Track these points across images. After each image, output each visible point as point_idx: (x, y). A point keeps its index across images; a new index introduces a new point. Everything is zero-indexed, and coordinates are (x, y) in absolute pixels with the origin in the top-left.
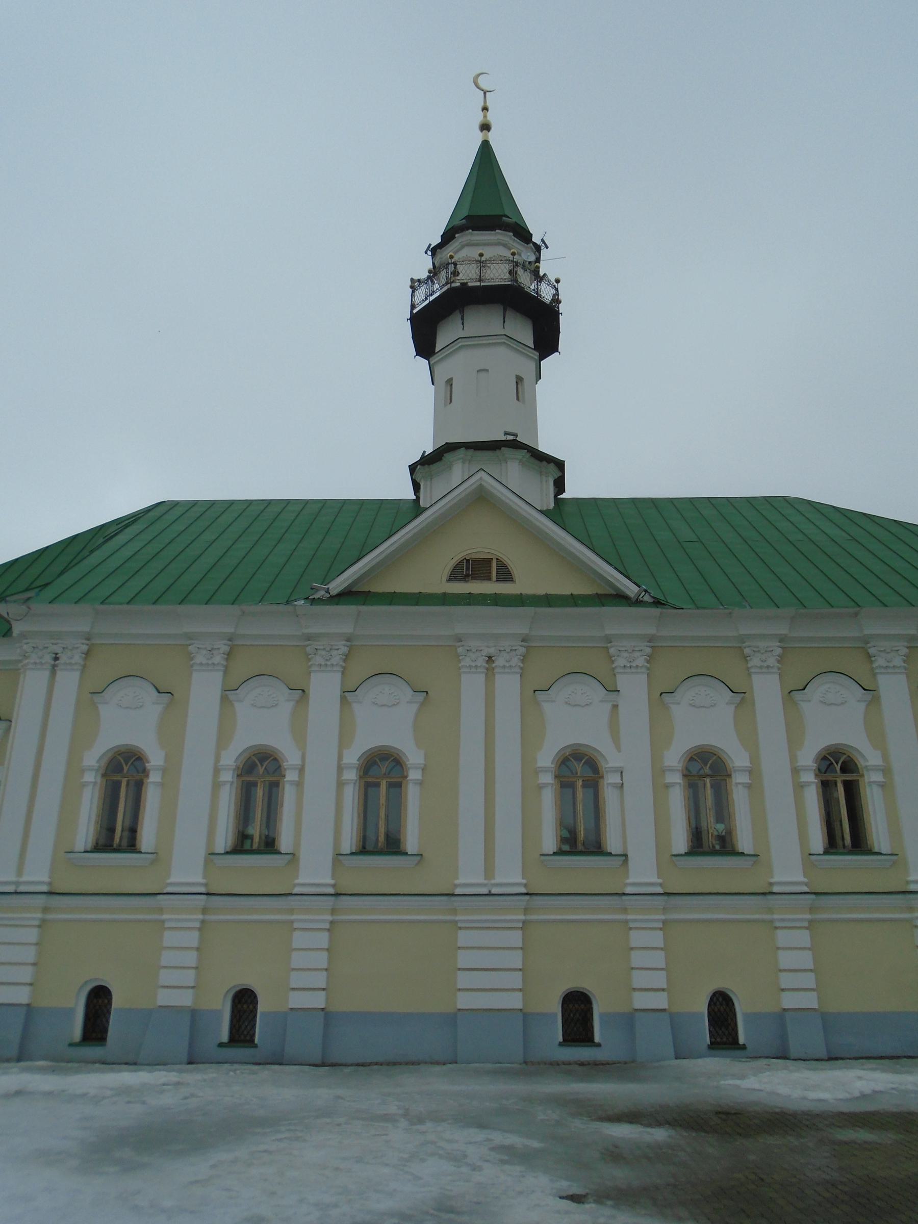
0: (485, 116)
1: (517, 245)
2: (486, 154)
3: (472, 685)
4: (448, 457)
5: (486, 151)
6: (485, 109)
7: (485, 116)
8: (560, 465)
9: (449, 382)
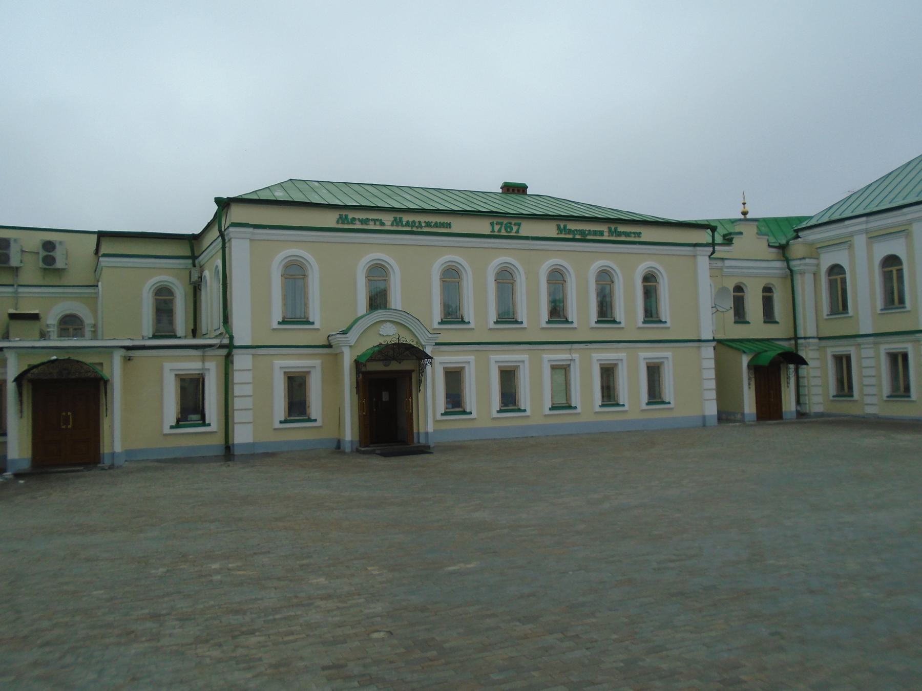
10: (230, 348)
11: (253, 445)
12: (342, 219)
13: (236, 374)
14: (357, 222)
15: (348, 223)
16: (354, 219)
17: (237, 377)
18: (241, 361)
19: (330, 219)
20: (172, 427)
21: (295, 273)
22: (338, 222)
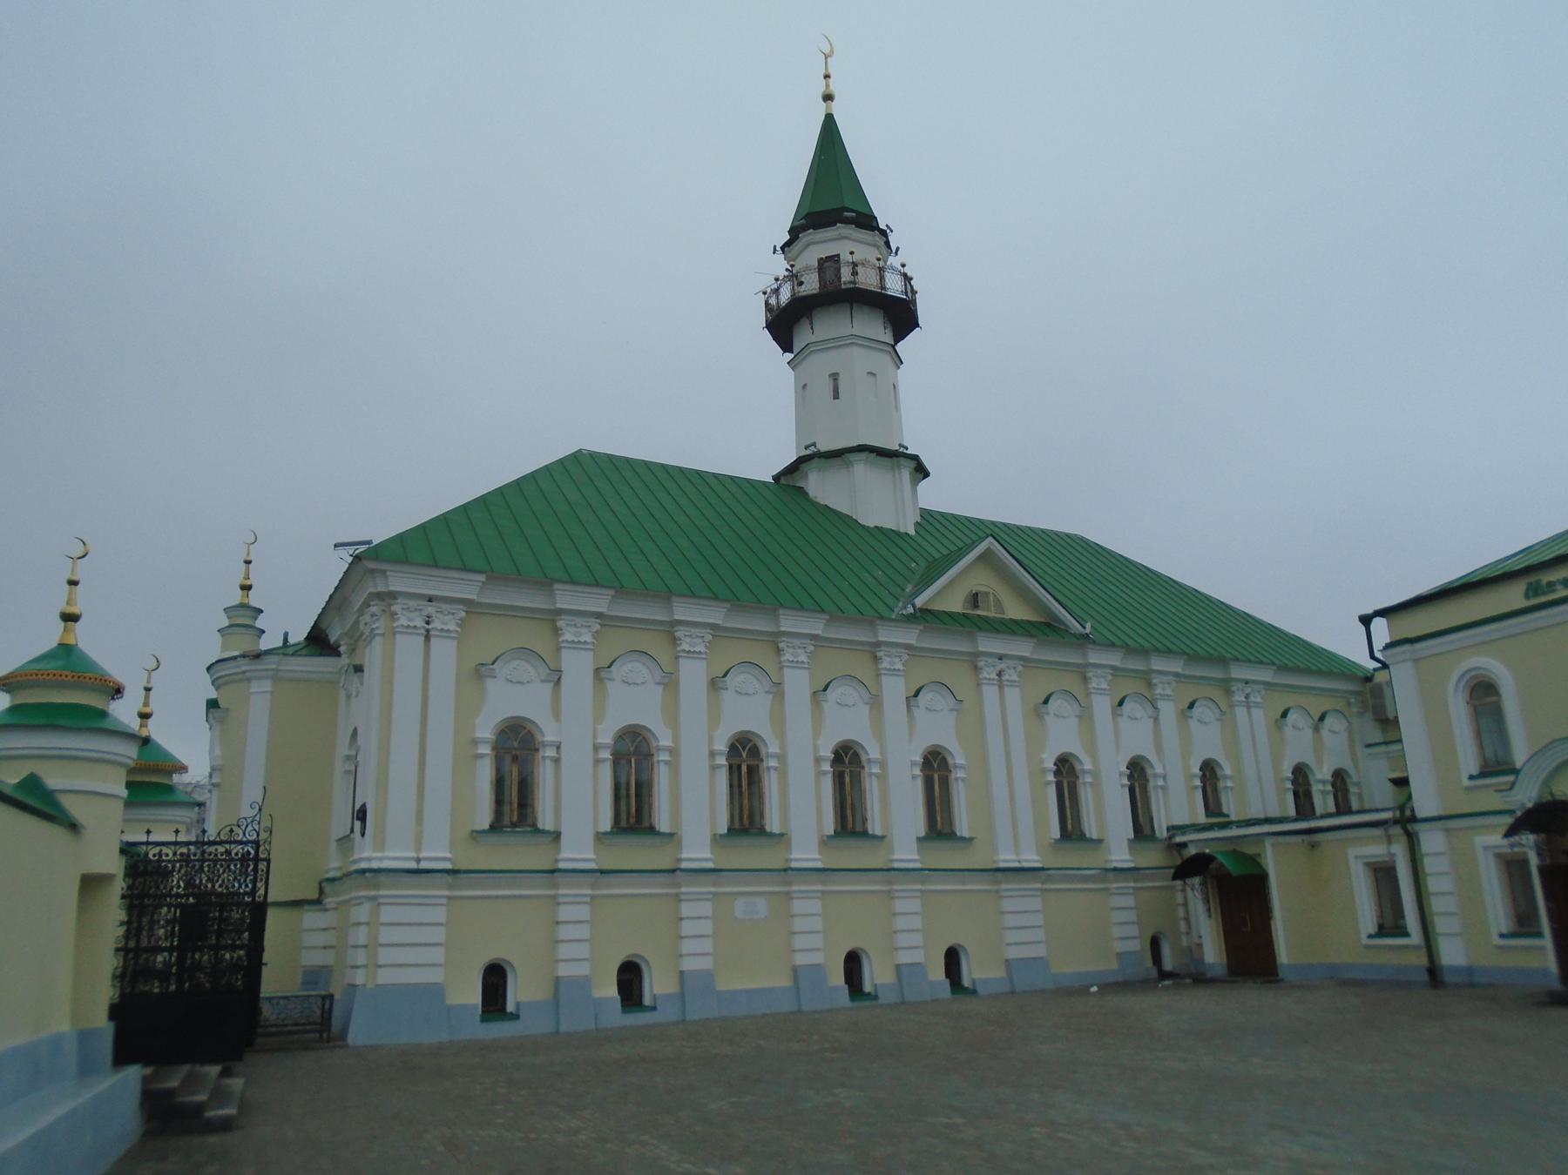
0: (827, 85)
1: (884, 249)
2: (830, 131)
3: (990, 693)
4: (852, 457)
5: (829, 126)
6: (827, 76)
7: (827, 85)
8: (926, 474)
9: (835, 377)
10: (1406, 821)
11: (1470, 970)
12: (1533, 590)
13: (1427, 861)
14: (1559, 587)
15: (1544, 593)
16: (1551, 585)
17: (1429, 865)
18: (1432, 841)
19: (1513, 596)
20: (1370, 936)
21: (1483, 692)
22: (1527, 596)
